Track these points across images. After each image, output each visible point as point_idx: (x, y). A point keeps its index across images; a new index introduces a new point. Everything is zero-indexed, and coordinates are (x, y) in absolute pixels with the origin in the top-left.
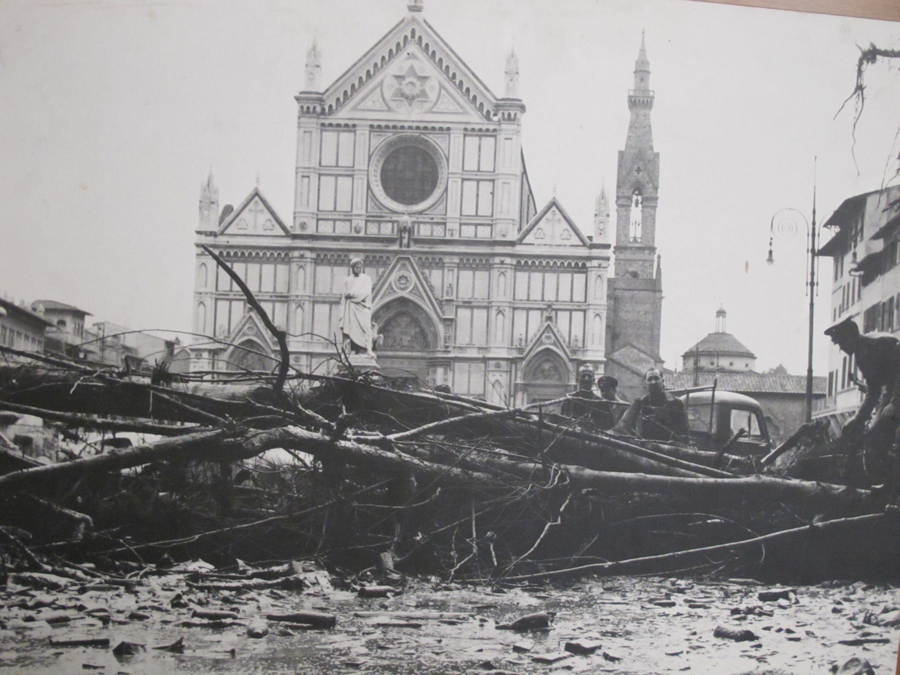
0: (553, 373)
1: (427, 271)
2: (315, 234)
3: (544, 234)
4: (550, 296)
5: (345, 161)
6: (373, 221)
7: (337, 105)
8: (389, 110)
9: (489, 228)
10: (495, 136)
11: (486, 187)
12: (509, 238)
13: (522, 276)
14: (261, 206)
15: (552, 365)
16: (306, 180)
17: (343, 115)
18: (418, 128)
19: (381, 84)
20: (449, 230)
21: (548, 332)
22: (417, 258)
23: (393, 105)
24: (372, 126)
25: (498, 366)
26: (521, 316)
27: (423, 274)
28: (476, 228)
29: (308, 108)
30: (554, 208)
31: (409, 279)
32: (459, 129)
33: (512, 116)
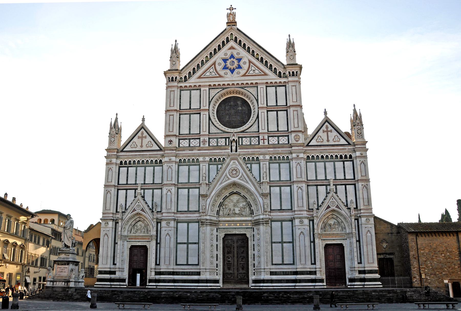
0: (337, 226)
1: (249, 165)
2: (178, 147)
3: (323, 140)
4: (330, 177)
5: (195, 105)
6: (213, 138)
7: (189, 76)
8: (220, 76)
9: (287, 138)
10: (285, 86)
11: (282, 114)
12: (301, 141)
13: (311, 165)
14: (145, 134)
15: (336, 221)
16: (171, 117)
17: (193, 81)
18: (238, 84)
19: (214, 64)
20: (261, 140)
21: (332, 199)
22: (242, 158)
23: (222, 73)
24: (210, 85)
25: (301, 222)
26: (312, 190)
27: (247, 167)
28: (278, 138)
29: (173, 78)
30: (327, 124)
31: (237, 170)
32: (262, 83)
33: (295, 73)
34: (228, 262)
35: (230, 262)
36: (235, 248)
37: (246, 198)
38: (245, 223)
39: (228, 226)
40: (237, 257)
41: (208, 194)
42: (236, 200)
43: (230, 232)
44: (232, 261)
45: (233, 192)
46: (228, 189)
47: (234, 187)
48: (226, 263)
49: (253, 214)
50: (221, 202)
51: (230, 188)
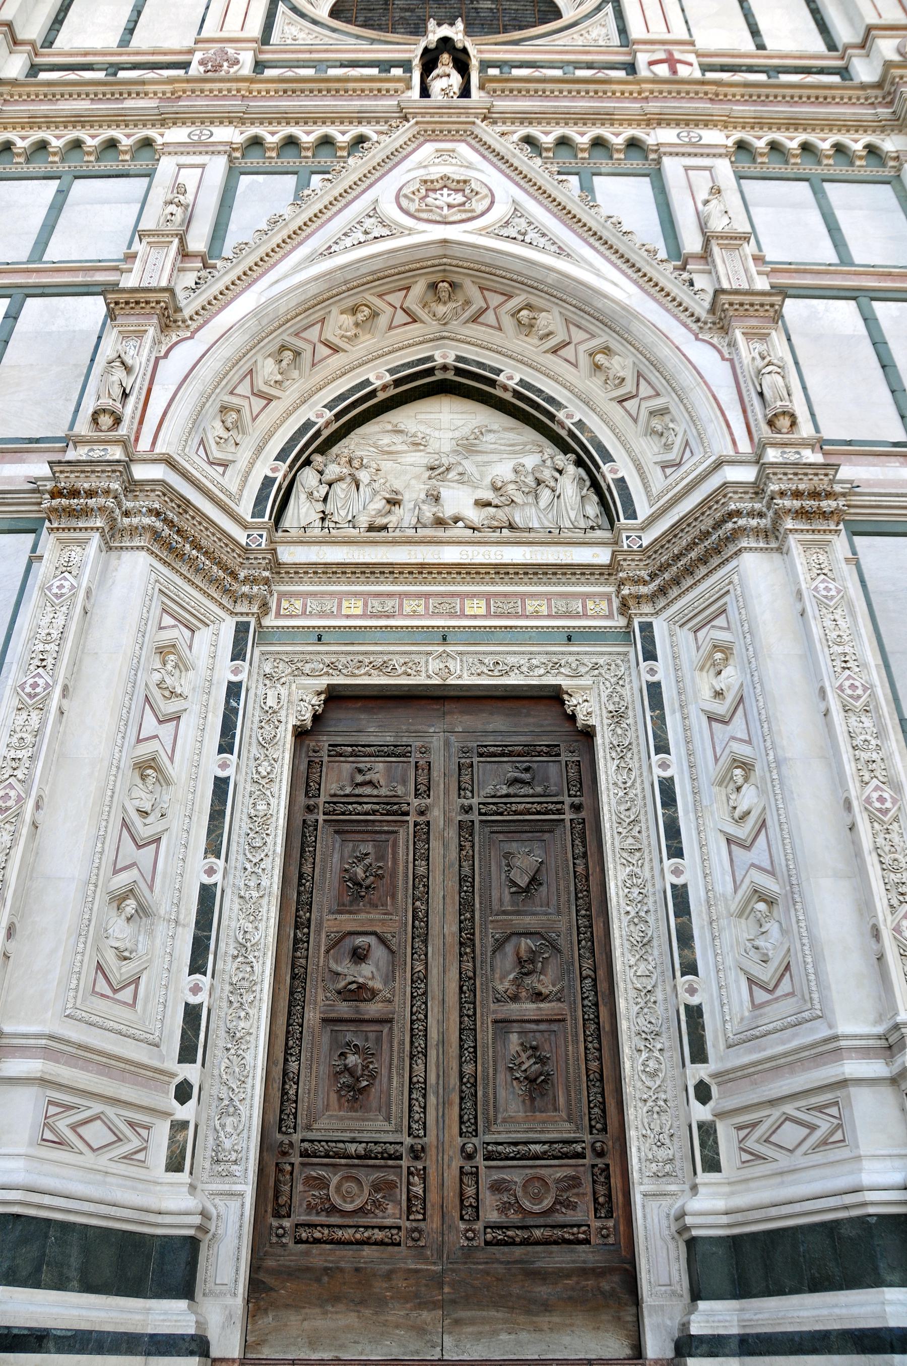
34: (344, 1009)
35: (373, 1009)
36: (435, 845)
37: (551, 400)
38: (548, 596)
39: (363, 616)
40: (466, 942)
41: (189, 306)
42: (457, 434)
43: (381, 668)
44: (403, 986)
45: (430, 359)
46: (383, 320)
47: (441, 309)
48: (312, 1016)
49: (631, 514)
50: (308, 424)
51: (401, 317)
